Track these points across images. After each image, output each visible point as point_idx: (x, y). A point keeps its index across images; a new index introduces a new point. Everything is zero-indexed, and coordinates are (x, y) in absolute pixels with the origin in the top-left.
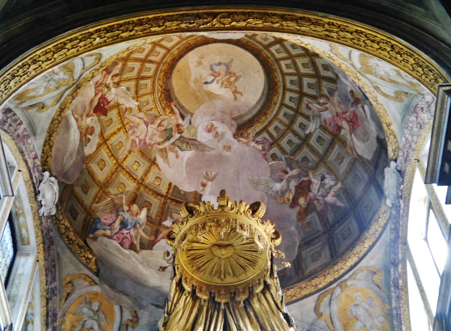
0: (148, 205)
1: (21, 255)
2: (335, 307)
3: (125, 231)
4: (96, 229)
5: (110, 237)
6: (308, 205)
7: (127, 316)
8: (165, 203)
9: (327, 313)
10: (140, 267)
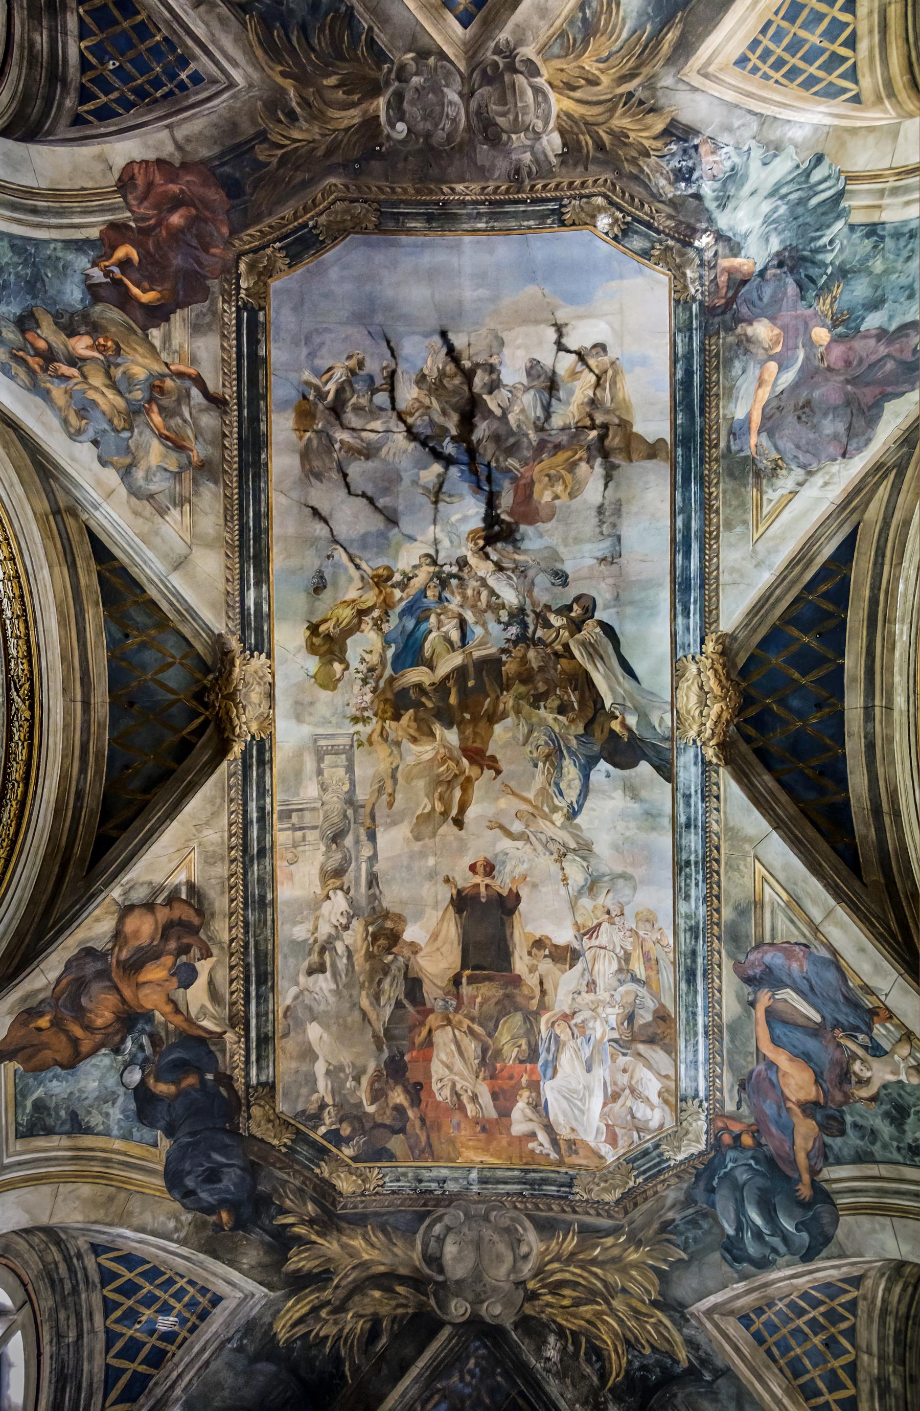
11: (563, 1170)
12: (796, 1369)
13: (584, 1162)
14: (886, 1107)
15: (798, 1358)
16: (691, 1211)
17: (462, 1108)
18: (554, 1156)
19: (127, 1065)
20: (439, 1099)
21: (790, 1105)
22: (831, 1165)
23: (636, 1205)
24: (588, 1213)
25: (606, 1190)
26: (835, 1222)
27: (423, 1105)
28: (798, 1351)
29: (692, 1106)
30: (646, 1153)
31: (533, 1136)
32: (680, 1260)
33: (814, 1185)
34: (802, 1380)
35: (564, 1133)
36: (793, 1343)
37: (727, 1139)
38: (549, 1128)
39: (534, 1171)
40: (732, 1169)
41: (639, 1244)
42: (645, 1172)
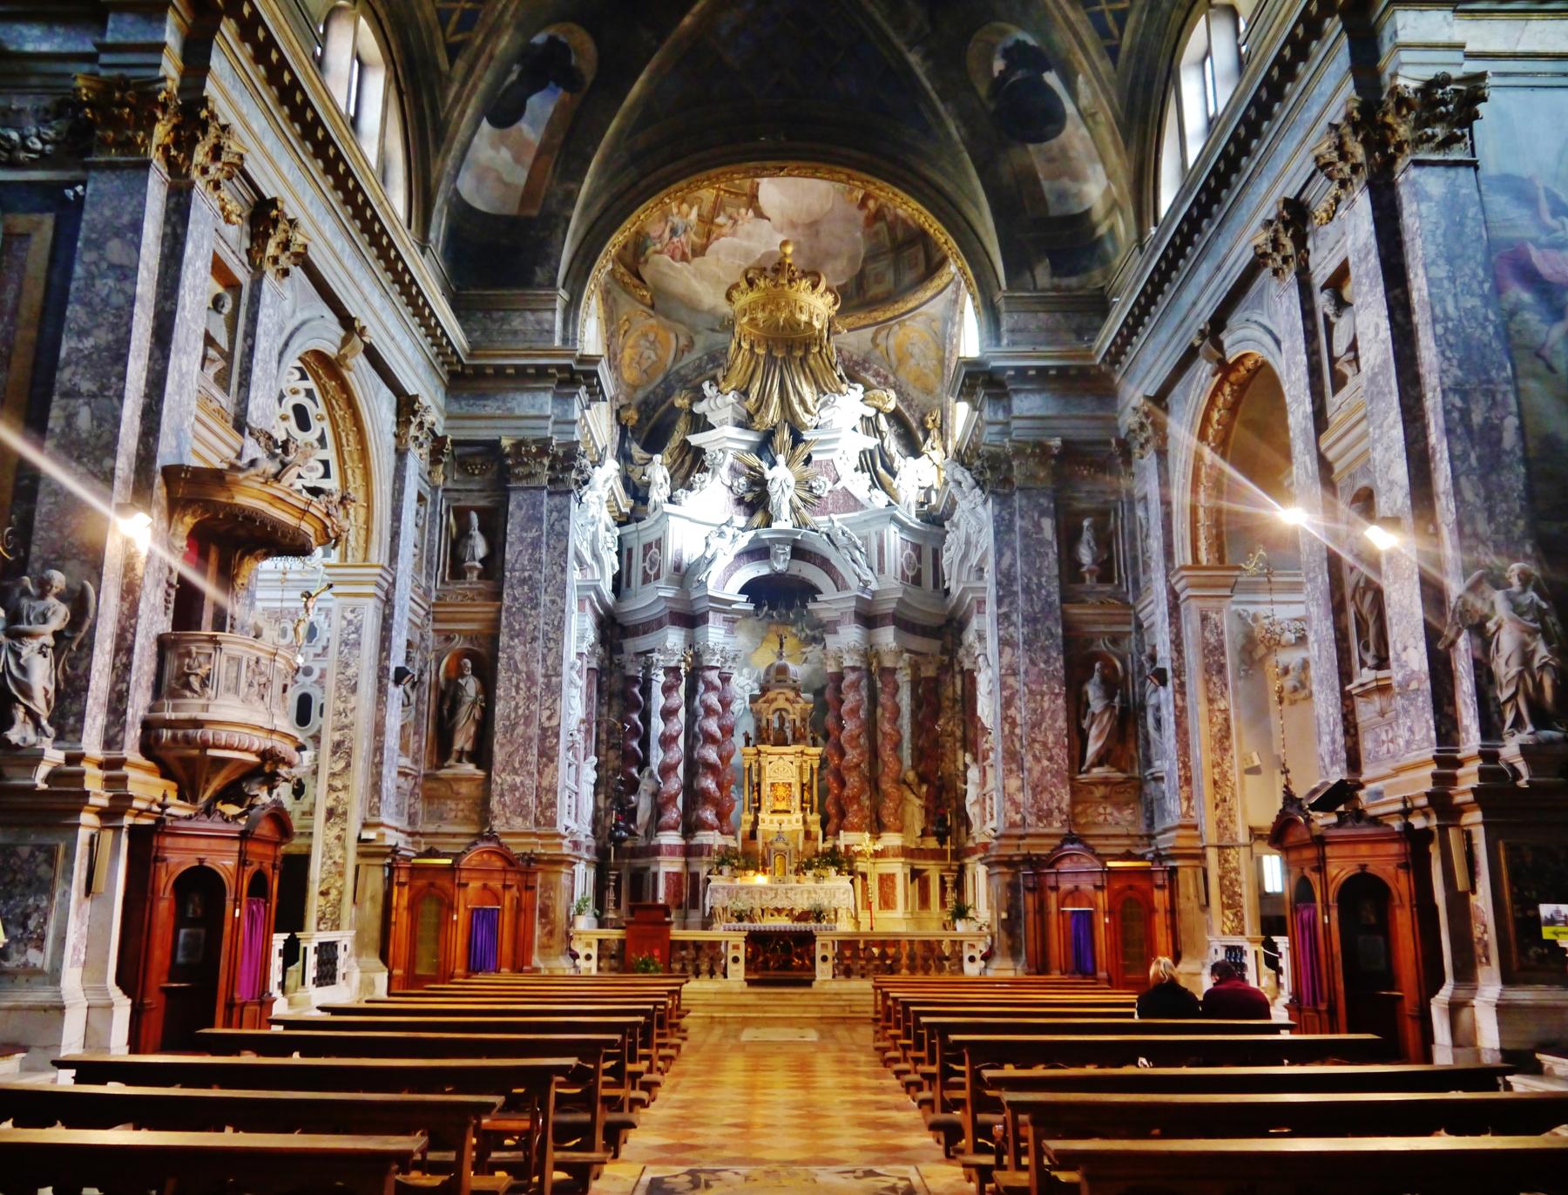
2: (892, 341)
3: (675, 240)
5: (660, 252)
7: (683, 341)
9: (882, 347)
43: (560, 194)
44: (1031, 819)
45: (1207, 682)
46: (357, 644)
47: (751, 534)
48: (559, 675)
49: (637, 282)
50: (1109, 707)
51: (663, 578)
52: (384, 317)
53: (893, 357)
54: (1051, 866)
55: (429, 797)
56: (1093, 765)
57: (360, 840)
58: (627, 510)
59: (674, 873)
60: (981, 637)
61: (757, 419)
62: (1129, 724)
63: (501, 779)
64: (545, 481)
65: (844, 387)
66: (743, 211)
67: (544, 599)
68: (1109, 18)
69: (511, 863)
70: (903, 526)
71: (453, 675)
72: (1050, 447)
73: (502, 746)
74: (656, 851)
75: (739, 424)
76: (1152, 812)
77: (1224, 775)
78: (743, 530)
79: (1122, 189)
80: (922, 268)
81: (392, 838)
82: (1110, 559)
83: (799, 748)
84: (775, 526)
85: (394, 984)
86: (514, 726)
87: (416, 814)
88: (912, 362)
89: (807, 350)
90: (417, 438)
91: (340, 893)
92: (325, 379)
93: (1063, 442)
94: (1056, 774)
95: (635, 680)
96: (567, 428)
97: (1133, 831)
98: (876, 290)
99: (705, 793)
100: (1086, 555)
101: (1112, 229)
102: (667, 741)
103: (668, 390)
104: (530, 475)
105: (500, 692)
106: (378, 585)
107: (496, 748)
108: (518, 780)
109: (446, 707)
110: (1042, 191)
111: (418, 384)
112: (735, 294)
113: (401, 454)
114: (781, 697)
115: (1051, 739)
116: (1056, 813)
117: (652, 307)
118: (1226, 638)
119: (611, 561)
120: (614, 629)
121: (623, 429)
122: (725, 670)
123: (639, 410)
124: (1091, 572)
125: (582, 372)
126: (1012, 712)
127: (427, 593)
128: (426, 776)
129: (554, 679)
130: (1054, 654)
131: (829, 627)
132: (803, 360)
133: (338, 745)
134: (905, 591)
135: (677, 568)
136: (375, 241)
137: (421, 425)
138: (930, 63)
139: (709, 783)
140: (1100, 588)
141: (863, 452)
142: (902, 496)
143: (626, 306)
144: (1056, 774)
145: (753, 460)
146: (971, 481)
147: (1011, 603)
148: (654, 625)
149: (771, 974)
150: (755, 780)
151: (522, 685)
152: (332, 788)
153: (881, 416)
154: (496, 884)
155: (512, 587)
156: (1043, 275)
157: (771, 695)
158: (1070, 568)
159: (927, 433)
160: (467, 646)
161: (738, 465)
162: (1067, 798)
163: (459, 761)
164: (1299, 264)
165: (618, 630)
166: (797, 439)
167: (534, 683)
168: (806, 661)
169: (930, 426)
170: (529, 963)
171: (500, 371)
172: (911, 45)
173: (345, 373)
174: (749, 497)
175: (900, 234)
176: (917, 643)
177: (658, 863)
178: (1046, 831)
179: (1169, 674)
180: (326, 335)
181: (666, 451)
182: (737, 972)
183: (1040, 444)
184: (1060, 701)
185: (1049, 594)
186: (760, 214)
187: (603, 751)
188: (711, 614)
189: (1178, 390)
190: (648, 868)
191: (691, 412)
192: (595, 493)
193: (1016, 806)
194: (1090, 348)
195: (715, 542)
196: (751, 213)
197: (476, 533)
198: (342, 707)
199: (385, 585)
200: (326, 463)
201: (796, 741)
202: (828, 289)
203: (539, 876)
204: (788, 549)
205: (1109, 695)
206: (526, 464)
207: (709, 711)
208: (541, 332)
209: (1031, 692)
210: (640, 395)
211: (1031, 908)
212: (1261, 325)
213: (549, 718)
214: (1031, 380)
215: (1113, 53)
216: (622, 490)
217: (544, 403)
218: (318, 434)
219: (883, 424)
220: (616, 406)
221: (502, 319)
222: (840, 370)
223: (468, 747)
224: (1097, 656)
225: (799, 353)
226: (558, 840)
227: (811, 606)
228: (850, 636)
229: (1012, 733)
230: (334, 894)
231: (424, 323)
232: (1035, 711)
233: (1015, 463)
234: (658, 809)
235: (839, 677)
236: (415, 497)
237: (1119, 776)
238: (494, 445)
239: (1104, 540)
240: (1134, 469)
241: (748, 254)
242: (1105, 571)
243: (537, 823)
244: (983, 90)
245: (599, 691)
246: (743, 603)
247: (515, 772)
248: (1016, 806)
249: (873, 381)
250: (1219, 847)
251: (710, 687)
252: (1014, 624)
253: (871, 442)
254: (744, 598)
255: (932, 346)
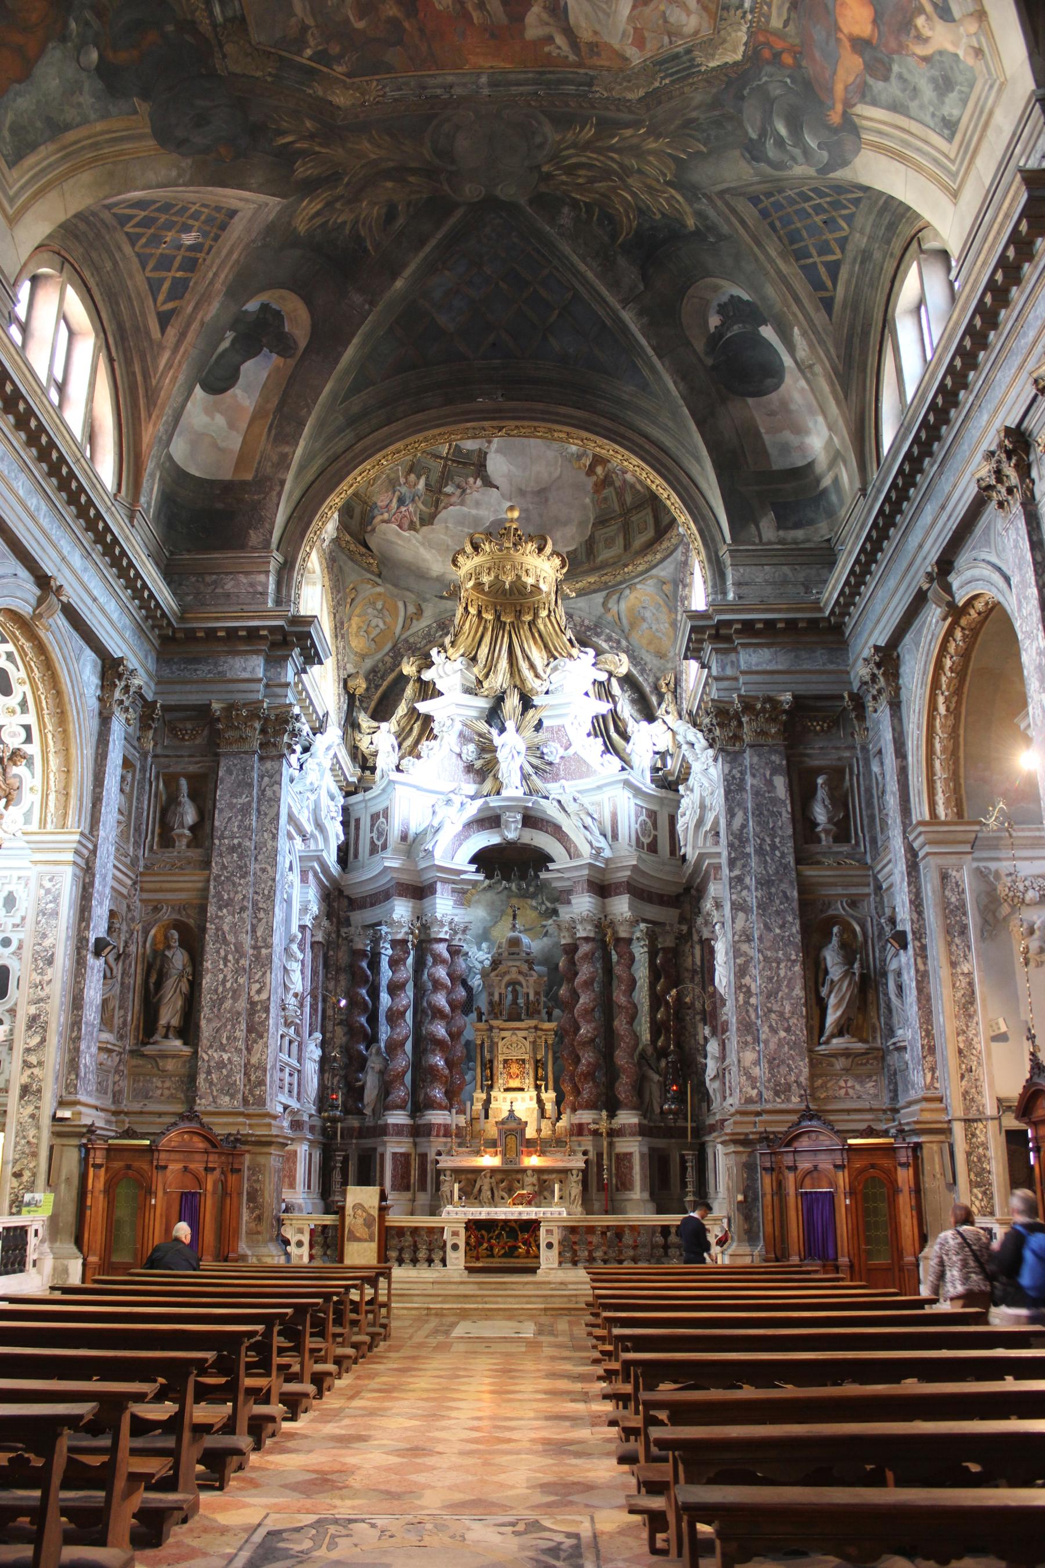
0: (427, 471)
1: (307, 583)
2: (623, 605)
3: (403, 509)
4: (374, 518)
6: (607, 476)
7: (411, 609)
8: (445, 466)
9: (614, 609)
10: (422, 550)
11: (582, 71)
12: (793, 237)
13: (607, 64)
14: (935, 73)
15: (798, 230)
16: (717, 113)
17: (467, 16)
18: (572, 58)
19: (79, 49)
20: (439, 7)
21: (840, 36)
22: (866, 103)
23: (660, 103)
24: (607, 109)
25: (630, 89)
26: (857, 151)
27: (422, 15)
28: (799, 225)
29: (735, 16)
30: (676, 57)
31: (550, 39)
32: (699, 153)
33: (845, 113)
34: (796, 246)
35: (586, 35)
36: (795, 218)
37: (766, 54)
38: (569, 33)
39: (550, 72)
40: (766, 83)
41: (658, 136)
42: (672, 75)
43: (275, 458)
44: (767, 1094)
45: (949, 944)
46: (55, 914)
47: (480, 802)
48: (269, 946)
49: (364, 550)
50: (848, 973)
51: (389, 850)
52: (85, 578)
53: (625, 621)
54: (788, 1144)
55: (135, 1075)
56: (833, 1036)
57: (54, 1118)
58: (355, 780)
59: (402, 1154)
60: (718, 905)
61: (486, 684)
62: (869, 989)
63: (208, 1055)
64: (256, 745)
65: (575, 652)
66: (471, 480)
67: (253, 867)
68: (822, 270)
69: (214, 1146)
70: (637, 791)
71: (161, 946)
72: (781, 702)
73: (209, 1020)
74: (383, 1130)
75: (468, 691)
76: (896, 1084)
77: (969, 1043)
78: (473, 798)
79: (843, 440)
80: (650, 533)
81: (89, 1117)
82: (847, 816)
83: (532, 1023)
84: (505, 793)
85: (89, 1273)
86: (222, 1000)
87: (120, 1092)
88: (645, 626)
89: (536, 615)
90: (121, 702)
91: (34, 1175)
92: (22, 641)
93: (795, 697)
94: (794, 1045)
95: (363, 954)
96: (278, 690)
97: (876, 1104)
98: (605, 555)
99: (433, 1070)
100: (820, 814)
101: (836, 480)
102: (394, 1017)
103: (397, 658)
104: (242, 739)
105: (208, 965)
106: (77, 852)
107: (203, 1023)
108: (225, 1056)
109: (153, 980)
110: (763, 444)
111: (124, 647)
112: (461, 559)
113: (105, 720)
114: (514, 969)
115: (788, 1008)
116: (794, 1087)
117: (379, 576)
118: (968, 896)
119: (335, 831)
120: (340, 902)
121: (351, 697)
122: (454, 943)
123: (367, 679)
124: (827, 832)
125: (295, 634)
126: (747, 980)
127: (134, 862)
128: (131, 1052)
129: (264, 951)
130: (790, 919)
131: (563, 897)
132: (532, 624)
133: (33, 1020)
134: (639, 858)
135: (404, 838)
136: (73, 499)
137: (126, 689)
138: (645, 320)
139: (439, 1061)
140: (837, 848)
141: (596, 717)
142: (635, 760)
143: (353, 575)
144: (794, 1045)
145: (483, 727)
146: (704, 743)
147: (744, 866)
148: (382, 897)
149: (496, 1262)
150: (487, 1056)
151: (230, 957)
152: (27, 1064)
153: (614, 680)
154: (197, 1166)
155: (221, 855)
156: (768, 529)
157: (502, 968)
158: (804, 827)
159: (661, 697)
160: (175, 916)
161: (467, 732)
162: (806, 1071)
163: (166, 1037)
164: (1024, 494)
165: (346, 902)
166: (527, 703)
167: (242, 955)
168: (546, 934)
169: (664, 690)
170: (235, 1250)
171: (211, 633)
172: (625, 303)
173: (42, 633)
174: (478, 764)
175: (629, 499)
176: (653, 912)
177: (384, 1143)
178: (784, 1106)
179: (910, 937)
180: (19, 595)
181: (394, 720)
182: (457, 1260)
183: (769, 699)
184: (797, 968)
185: (783, 855)
186: (488, 483)
187: (330, 1028)
188: (439, 885)
189: (908, 639)
190: (375, 1149)
191: (419, 679)
192: (316, 760)
193: (752, 1080)
194: (817, 601)
195: (442, 811)
196: (479, 482)
197: (185, 799)
198: (38, 978)
199: (86, 852)
200: (27, 728)
201: (530, 1015)
202: (555, 553)
203: (247, 1157)
204: (519, 817)
205: (849, 961)
206: (237, 728)
207: (437, 985)
208: (256, 593)
209: (766, 958)
210: (369, 664)
211: (768, 1190)
212: (989, 563)
213: (259, 992)
214: (757, 633)
215: (828, 304)
216: (348, 759)
217: (256, 666)
218: (21, 696)
219: (616, 688)
220: (343, 675)
221: (215, 582)
222: (569, 634)
223: (175, 1022)
224: (834, 920)
225: (528, 618)
226: (267, 1120)
227: (543, 875)
228: (583, 904)
229: (747, 1002)
230: (27, 1175)
231: (130, 584)
232: (770, 979)
233: (744, 719)
234: (386, 1088)
235: (571, 949)
236: (120, 761)
237: (860, 1046)
238: (204, 710)
239: (840, 801)
240: (869, 724)
241: (476, 521)
242: (842, 832)
243: (245, 1101)
244: (700, 346)
245: (326, 965)
246: (471, 873)
247: (222, 1048)
248: (752, 1080)
249: (605, 646)
250: (966, 1121)
251: (438, 960)
252: (747, 888)
253: (604, 707)
254: (473, 868)
255: (665, 609)
